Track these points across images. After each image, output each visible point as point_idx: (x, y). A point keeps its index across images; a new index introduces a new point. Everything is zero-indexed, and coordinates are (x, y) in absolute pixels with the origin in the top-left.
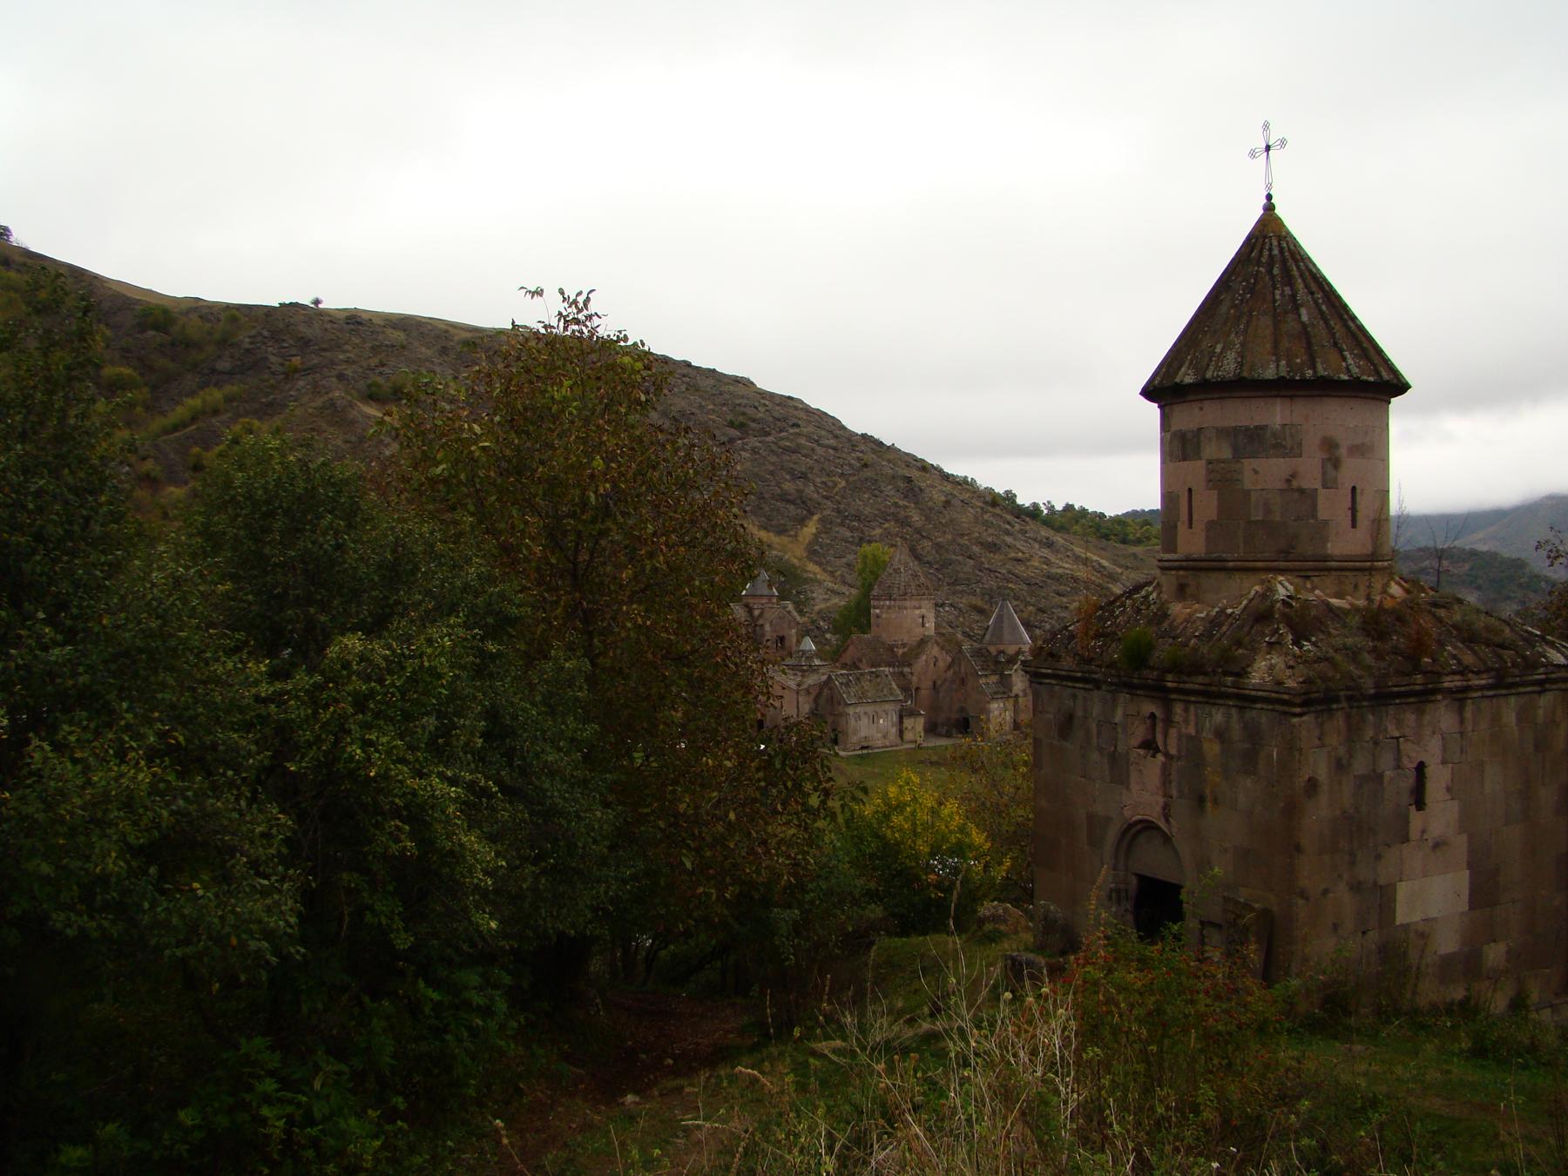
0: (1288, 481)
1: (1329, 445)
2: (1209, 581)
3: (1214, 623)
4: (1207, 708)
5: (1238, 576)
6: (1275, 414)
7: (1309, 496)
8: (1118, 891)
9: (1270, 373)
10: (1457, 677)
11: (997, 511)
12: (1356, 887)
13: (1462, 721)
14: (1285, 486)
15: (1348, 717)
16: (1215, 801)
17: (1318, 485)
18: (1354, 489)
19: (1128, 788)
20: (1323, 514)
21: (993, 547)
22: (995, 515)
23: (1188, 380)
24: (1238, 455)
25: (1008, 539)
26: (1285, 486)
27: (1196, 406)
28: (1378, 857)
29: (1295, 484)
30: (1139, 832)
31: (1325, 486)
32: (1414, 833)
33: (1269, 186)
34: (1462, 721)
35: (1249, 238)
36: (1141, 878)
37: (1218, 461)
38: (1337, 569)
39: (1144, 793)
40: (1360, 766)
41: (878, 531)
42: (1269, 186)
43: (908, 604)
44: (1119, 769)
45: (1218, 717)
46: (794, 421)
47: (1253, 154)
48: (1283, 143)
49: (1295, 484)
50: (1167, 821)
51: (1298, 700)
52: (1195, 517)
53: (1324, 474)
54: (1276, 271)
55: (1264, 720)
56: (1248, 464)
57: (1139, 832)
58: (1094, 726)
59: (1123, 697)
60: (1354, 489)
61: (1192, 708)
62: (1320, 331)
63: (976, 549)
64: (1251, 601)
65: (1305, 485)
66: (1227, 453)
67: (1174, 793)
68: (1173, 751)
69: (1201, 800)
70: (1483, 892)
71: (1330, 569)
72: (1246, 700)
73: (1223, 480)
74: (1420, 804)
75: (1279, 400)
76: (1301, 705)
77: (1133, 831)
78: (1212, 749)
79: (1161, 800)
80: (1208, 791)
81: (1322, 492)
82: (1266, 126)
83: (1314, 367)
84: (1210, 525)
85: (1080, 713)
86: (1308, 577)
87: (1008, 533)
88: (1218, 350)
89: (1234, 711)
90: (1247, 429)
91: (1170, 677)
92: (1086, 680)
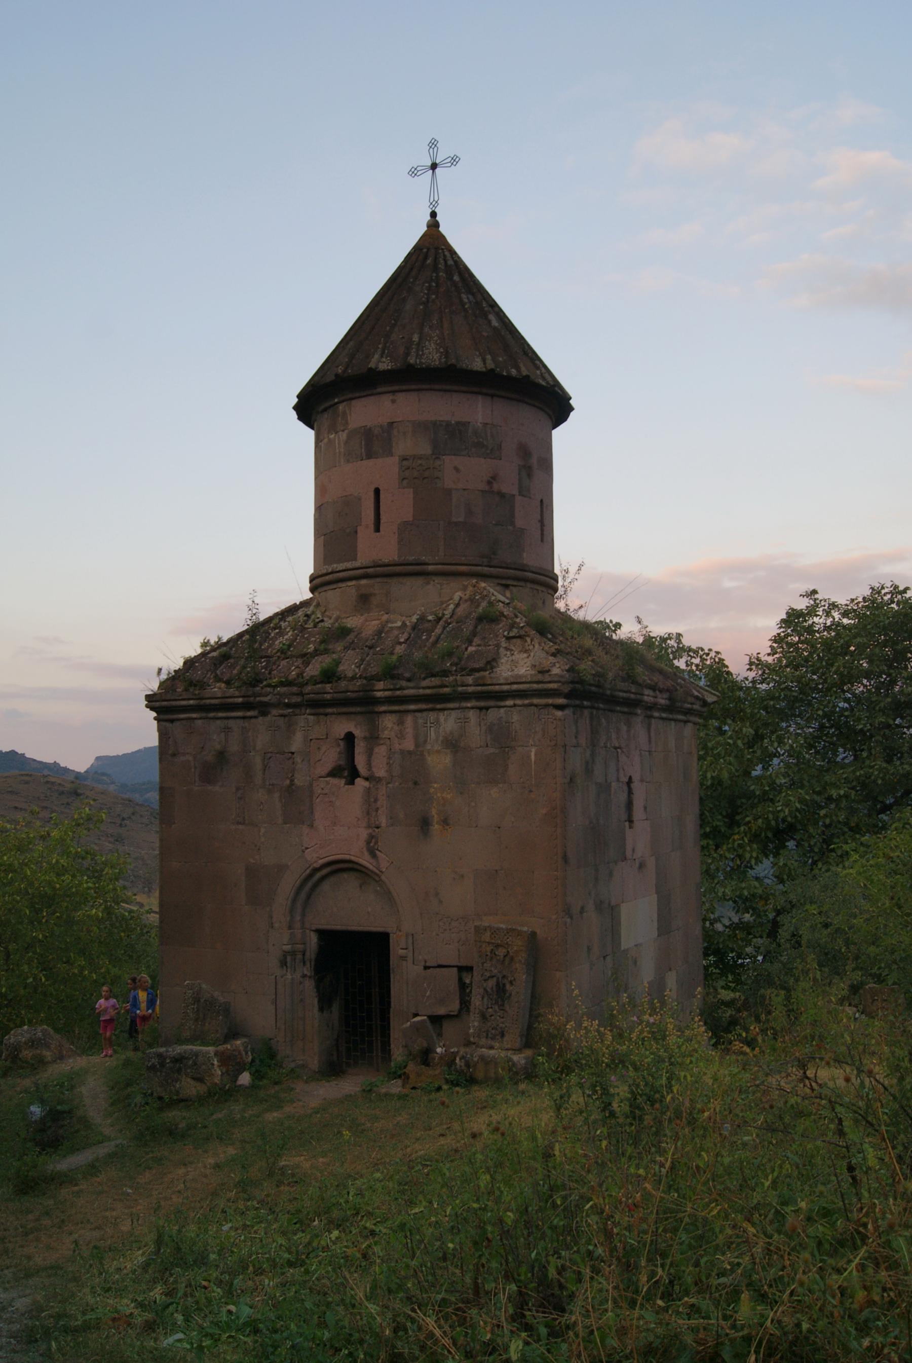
0: (489, 483)
4: (432, 716)
5: (437, 580)
6: (476, 411)
8: (293, 953)
9: (477, 365)
10: (651, 693)
12: (599, 906)
13: (650, 741)
14: (487, 488)
15: (591, 718)
16: (445, 822)
17: (515, 492)
18: (542, 501)
19: (311, 826)
20: (519, 523)
23: (385, 365)
26: (487, 488)
27: (391, 397)
28: (611, 874)
29: (496, 487)
30: (323, 878)
31: (521, 494)
32: (629, 853)
33: (434, 203)
34: (650, 741)
35: (417, 249)
36: (321, 933)
37: (415, 457)
38: (533, 582)
39: (339, 824)
42: (434, 203)
44: (297, 805)
45: (448, 722)
47: (414, 172)
48: (454, 160)
49: (496, 487)
50: (373, 854)
51: (566, 689)
52: (383, 519)
53: (520, 480)
54: (456, 278)
55: (515, 718)
56: (449, 462)
57: (323, 878)
58: (258, 761)
59: (305, 719)
60: (542, 501)
61: (409, 720)
64: (457, 605)
65: (504, 491)
66: (425, 448)
67: (383, 821)
68: (381, 773)
69: (425, 824)
71: (526, 580)
72: (493, 697)
73: (419, 476)
74: (631, 821)
75: (480, 397)
76: (567, 696)
77: (318, 875)
78: (439, 762)
79: (364, 834)
80: (434, 812)
81: (518, 498)
82: (433, 144)
83: (518, 368)
84: (404, 527)
85: (234, 747)
86: (507, 586)
88: (416, 338)
89: (472, 714)
90: (448, 424)
91: (381, 685)
92: (247, 706)
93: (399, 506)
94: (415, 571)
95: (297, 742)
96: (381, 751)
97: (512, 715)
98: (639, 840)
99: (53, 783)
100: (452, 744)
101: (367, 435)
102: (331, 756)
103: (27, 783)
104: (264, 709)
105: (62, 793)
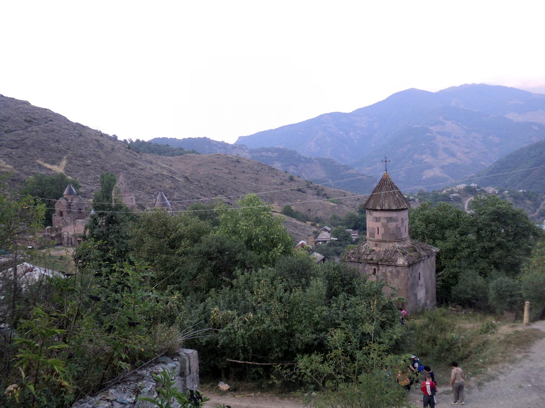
1: (402, 219)
2: (382, 244)
3: (386, 251)
6: (394, 215)
7: (399, 228)
9: (394, 208)
11: (130, 150)
21: (133, 165)
22: (130, 153)
23: (379, 209)
24: (388, 222)
25: (137, 161)
40: (413, 275)
41: (89, 161)
42: (386, 168)
43: (126, 194)
45: (390, 269)
46: (49, 119)
56: (390, 223)
59: (368, 265)
62: (400, 199)
63: (126, 166)
66: (386, 222)
70: (427, 292)
73: (385, 226)
78: (389, 274)
82: (386, 157)
84: (383, 234)
87: (136, 159)
93: (382, 231)
94: (385, 241)
95: (366, 269)
96: (380, 272)
97: (400, 269)
98: (421, 282)
99: (229, 158)
100: (391, 272)
101: (376, 218)
102: (372, 271)
103: (219, 158)
104: (361, 263)
105: (233, 162)
